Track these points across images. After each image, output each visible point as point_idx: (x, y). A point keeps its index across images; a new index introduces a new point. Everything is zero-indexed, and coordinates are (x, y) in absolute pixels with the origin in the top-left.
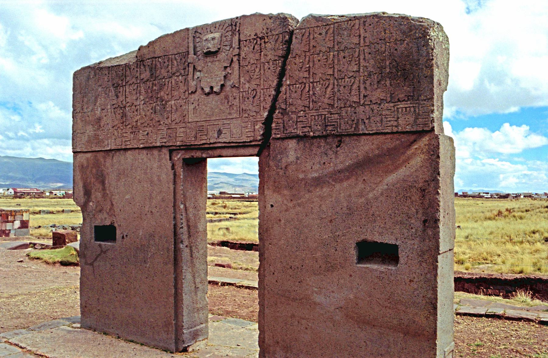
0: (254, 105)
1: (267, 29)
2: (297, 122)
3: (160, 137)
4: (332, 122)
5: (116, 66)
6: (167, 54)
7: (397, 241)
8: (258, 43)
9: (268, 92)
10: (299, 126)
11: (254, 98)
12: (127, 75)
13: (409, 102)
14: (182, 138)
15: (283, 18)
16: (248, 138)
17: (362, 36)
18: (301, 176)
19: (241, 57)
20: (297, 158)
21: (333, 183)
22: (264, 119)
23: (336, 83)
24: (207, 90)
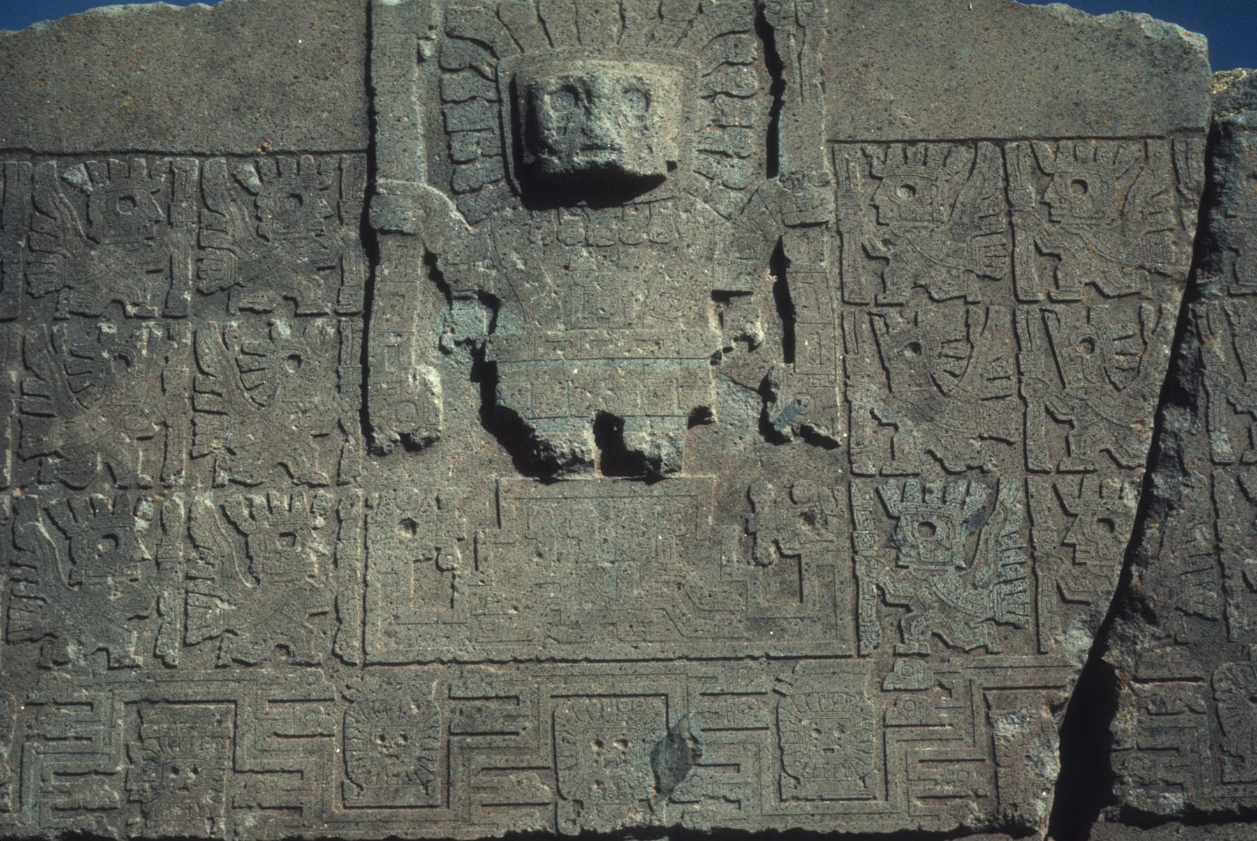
0: (983, 573)
3: (50, 764)
9: (1087, 493)
11: (977, 521)
14: (295, 781)
15: (1165, 48)
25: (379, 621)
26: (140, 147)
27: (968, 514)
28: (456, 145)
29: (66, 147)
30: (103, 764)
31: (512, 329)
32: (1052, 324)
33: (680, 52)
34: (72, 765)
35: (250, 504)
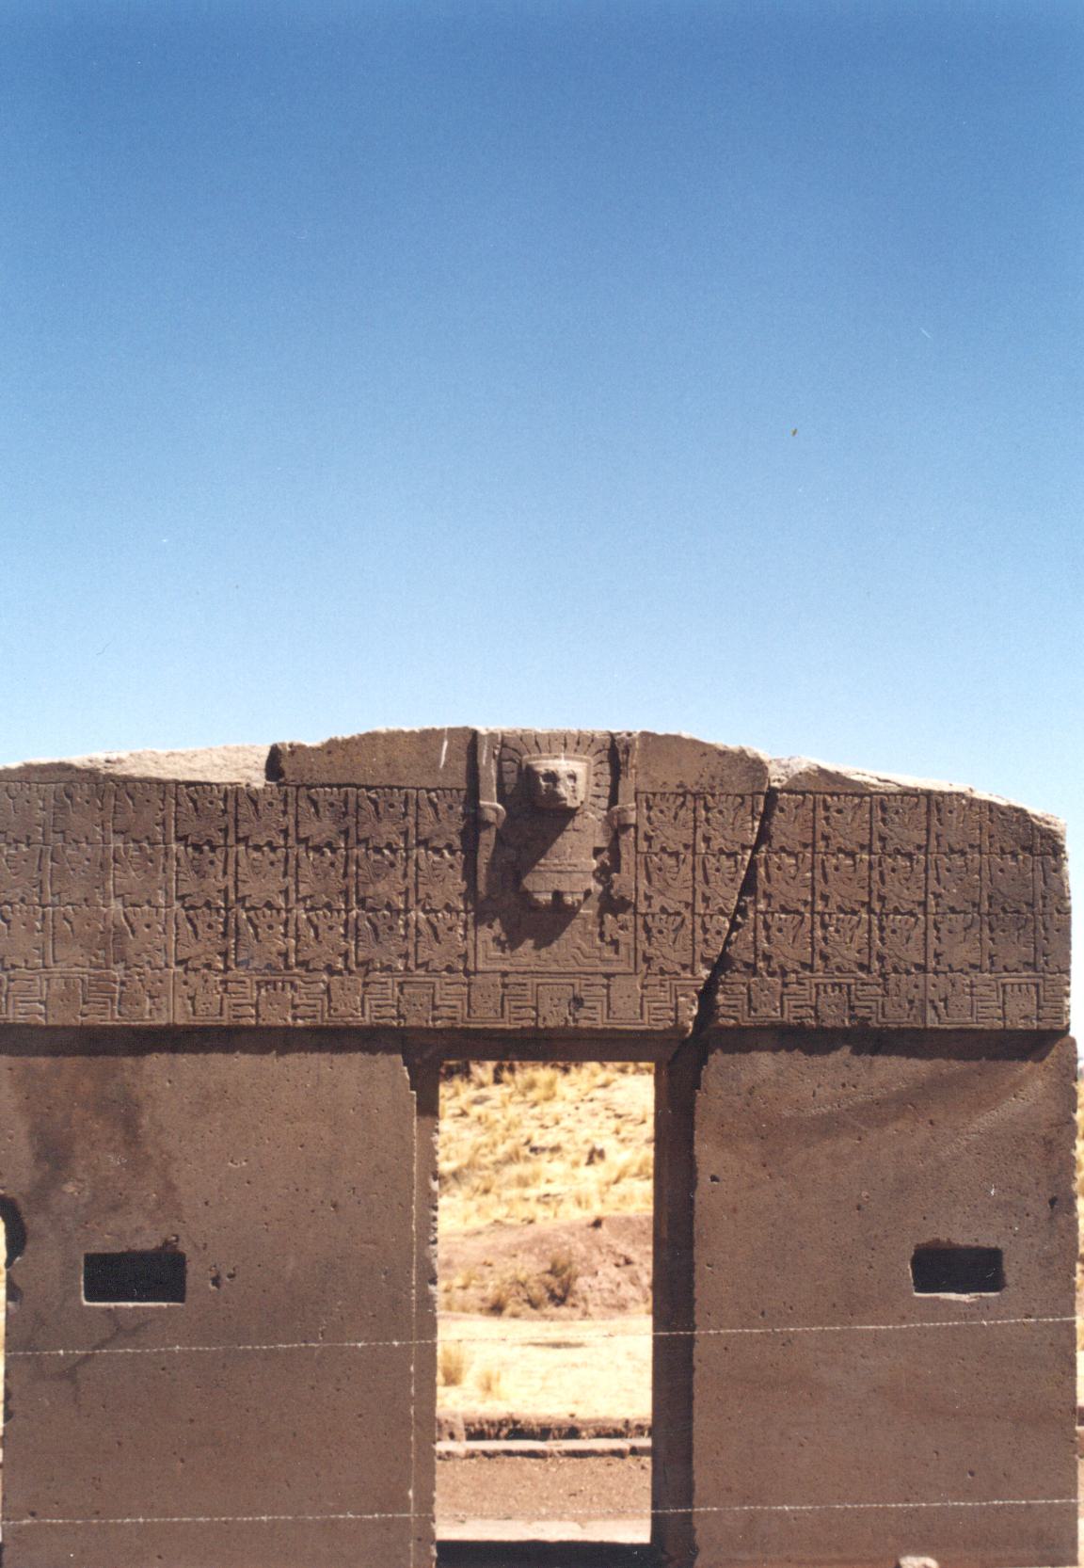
1: (713, 778)
2: (782, 995)
3: (373, 1002)
4: (865, 1001)
5: (189, 784)
6: (401, 784)
7: (999, 1242)
8: (690, 804)
10: (786, 1003)
12: (240, 817)
13: (1024, 974)
16: (660, 1023)
17: (933, 830)
19: (641, 835)
20: (779, 1073)
21: (863, 1128)
22: (702, 982)
24: (545, 898)
25: (481, 955)
26: (396, 784)
27: (674, 927)
30: (390, 1002)
32: (707, 862)
33: (585, 757)
34: (380, 1002)
35: (437, 917)
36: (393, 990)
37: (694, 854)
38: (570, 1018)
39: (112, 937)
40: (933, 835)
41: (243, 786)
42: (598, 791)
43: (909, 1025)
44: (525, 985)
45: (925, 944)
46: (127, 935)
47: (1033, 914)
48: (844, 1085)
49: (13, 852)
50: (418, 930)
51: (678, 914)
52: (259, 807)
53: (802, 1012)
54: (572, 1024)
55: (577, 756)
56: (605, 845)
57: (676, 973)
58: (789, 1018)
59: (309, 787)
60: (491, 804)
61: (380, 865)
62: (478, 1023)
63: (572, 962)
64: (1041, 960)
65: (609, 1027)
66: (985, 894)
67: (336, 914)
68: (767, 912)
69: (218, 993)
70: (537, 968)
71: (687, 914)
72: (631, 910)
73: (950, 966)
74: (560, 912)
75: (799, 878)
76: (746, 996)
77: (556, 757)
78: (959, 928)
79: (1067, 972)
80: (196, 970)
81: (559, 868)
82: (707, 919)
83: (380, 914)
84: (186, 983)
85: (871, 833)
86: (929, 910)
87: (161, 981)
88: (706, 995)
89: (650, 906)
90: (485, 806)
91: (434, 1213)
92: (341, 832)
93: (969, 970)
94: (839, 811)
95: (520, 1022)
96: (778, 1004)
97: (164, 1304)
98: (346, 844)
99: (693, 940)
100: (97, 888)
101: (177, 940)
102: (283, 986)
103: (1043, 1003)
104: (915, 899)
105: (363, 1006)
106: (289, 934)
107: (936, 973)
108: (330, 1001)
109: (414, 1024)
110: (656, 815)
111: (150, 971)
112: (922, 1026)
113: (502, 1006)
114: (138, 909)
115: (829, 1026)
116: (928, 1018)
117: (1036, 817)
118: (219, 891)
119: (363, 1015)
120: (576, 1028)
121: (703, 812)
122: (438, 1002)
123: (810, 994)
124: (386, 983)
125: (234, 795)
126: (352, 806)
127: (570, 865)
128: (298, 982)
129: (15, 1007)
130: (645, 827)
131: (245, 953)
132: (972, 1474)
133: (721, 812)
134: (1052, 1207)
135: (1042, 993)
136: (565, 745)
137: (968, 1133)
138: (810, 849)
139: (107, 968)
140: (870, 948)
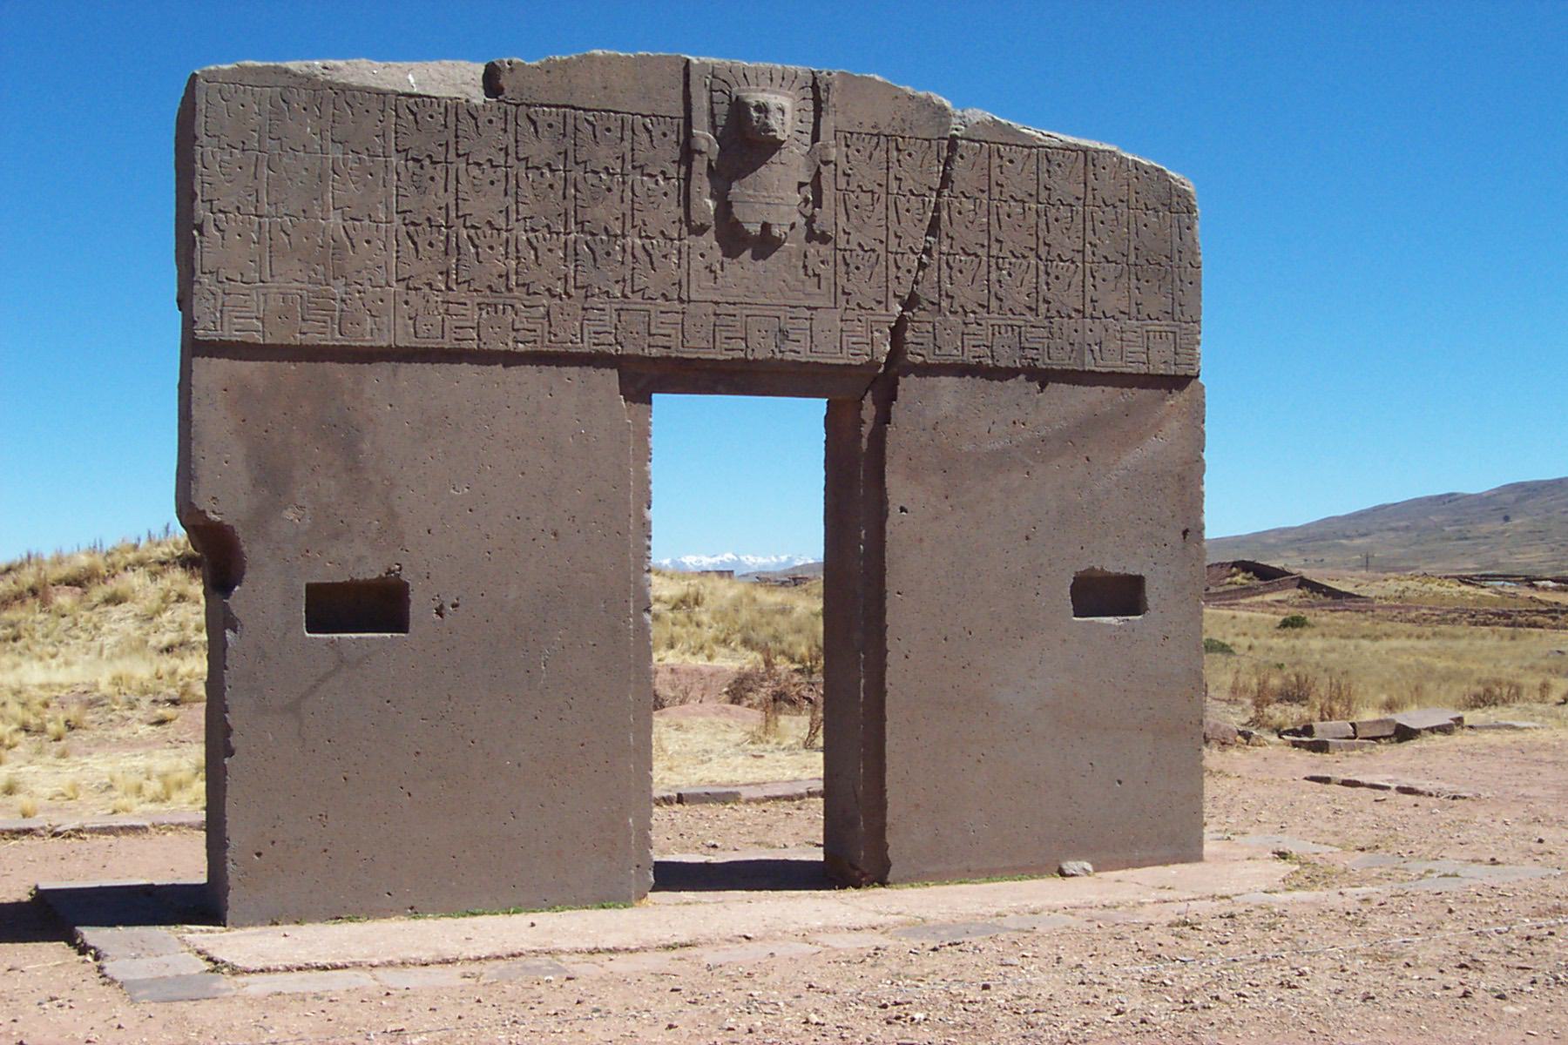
5: (410, 96)
8: (883, 145)
10: (966, 343)
12: (460, 133)
15: (939, 108)
16: (857, 357)
18: (967, 447)
19: (840, 172)
20: (959, 410)
21: (1032, 463)
23: (1042, 268)
24: (755, 229)
25: (693, 286)
28: (717, 119)
29: (587, 107)
31: (737, 190)
33: (790, 93)
36: (611, 317)
37: (888, 193)
38: (776, 350)
39: (331, 251)
40: (1089, 189)
41: (463, 101)
42: (801, 127)
43: (1070, 368)
44: (735, 316)
45: (1083, 291)
46: (348, 251)
47: (1171, 266)
48: (1014, 423)
49: (227, 158)
50: (634, 257)
51: (873, 250)
52: (479, 124)
53: (980, 351)
54: (779, 356)
55: (782, 90)
56: (809, 181)
57: (872, 309)
58: (969, 358)
59: (529, 106)
60: (703, 135)
61: (598, 190)
62: (691, 352)
63: (778, 293)
64: (1178, 309)
65: (811, 360)
66: (1132, 248)
67: (555, 236)
68: (949, 254)
69: (440, 314)
70: (748, 300)
71: (880, 249)
72: (831, 245)
73: (1104, 312)
74: (766, 244)
75: (977, 222)
76: (932, 335)
77: (764, 90)
78: (1110, 278)
79: (1198, 322)
80: (416, 289)
81: (768, 200)
82: (899, 257)
83: (597, 238)
84: (407, 303)
85: (1038, 184)
86: (1086, 259)
87: (382, 301)
88: (897, 332)
89: (848, 242)
90: (698, 135)
91: (648, 543)
92: (560, 154)
93: (1118, 315)
94: (1011, 161)
95: (730, 353)
96: (959, 344)
97: (388, 635)
98: (565, 167)
99: (887, 277)
100: (316, 199)
101: (397, 257)
102: (504, 309)
103: (1179, 350)
104: (1076, 248)
105: (582, 330)
106: (510, 256)
107: (1092, 318)
108: (550, 325)
109: (631, 352)
110: (854, 155)
111: (371, 289)
112: (1081, 369)
113: (714, 337)
114: (358, 223)
115: (1003, 366)
116: (1086, 359)
117: (1173, 178)
118: (440, 208)
119: (582, 341)
120: (782, 360)
121: (895, 153)
122: (653, 332)
123: (987, 335)
124: (604, 310)
125: (454, 110)
126: (570, 129)
127: (777, 198)
128: (519, 306)
129: (230, 323)
130: (843, 165)
131: (464, 273)
132: (1120, 782)
133: (910, 155)
134: (1185, 538)
135: (1178, 340)
136: (771, 80)
137: (1117, 470)
138: (986, 195)
139: (328, 285)
140: (1037, 292)
